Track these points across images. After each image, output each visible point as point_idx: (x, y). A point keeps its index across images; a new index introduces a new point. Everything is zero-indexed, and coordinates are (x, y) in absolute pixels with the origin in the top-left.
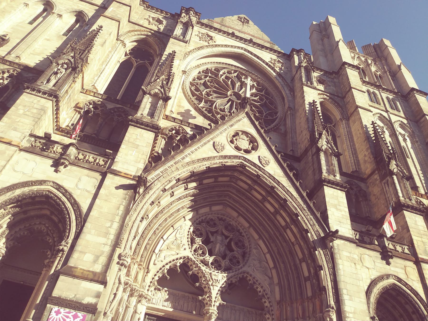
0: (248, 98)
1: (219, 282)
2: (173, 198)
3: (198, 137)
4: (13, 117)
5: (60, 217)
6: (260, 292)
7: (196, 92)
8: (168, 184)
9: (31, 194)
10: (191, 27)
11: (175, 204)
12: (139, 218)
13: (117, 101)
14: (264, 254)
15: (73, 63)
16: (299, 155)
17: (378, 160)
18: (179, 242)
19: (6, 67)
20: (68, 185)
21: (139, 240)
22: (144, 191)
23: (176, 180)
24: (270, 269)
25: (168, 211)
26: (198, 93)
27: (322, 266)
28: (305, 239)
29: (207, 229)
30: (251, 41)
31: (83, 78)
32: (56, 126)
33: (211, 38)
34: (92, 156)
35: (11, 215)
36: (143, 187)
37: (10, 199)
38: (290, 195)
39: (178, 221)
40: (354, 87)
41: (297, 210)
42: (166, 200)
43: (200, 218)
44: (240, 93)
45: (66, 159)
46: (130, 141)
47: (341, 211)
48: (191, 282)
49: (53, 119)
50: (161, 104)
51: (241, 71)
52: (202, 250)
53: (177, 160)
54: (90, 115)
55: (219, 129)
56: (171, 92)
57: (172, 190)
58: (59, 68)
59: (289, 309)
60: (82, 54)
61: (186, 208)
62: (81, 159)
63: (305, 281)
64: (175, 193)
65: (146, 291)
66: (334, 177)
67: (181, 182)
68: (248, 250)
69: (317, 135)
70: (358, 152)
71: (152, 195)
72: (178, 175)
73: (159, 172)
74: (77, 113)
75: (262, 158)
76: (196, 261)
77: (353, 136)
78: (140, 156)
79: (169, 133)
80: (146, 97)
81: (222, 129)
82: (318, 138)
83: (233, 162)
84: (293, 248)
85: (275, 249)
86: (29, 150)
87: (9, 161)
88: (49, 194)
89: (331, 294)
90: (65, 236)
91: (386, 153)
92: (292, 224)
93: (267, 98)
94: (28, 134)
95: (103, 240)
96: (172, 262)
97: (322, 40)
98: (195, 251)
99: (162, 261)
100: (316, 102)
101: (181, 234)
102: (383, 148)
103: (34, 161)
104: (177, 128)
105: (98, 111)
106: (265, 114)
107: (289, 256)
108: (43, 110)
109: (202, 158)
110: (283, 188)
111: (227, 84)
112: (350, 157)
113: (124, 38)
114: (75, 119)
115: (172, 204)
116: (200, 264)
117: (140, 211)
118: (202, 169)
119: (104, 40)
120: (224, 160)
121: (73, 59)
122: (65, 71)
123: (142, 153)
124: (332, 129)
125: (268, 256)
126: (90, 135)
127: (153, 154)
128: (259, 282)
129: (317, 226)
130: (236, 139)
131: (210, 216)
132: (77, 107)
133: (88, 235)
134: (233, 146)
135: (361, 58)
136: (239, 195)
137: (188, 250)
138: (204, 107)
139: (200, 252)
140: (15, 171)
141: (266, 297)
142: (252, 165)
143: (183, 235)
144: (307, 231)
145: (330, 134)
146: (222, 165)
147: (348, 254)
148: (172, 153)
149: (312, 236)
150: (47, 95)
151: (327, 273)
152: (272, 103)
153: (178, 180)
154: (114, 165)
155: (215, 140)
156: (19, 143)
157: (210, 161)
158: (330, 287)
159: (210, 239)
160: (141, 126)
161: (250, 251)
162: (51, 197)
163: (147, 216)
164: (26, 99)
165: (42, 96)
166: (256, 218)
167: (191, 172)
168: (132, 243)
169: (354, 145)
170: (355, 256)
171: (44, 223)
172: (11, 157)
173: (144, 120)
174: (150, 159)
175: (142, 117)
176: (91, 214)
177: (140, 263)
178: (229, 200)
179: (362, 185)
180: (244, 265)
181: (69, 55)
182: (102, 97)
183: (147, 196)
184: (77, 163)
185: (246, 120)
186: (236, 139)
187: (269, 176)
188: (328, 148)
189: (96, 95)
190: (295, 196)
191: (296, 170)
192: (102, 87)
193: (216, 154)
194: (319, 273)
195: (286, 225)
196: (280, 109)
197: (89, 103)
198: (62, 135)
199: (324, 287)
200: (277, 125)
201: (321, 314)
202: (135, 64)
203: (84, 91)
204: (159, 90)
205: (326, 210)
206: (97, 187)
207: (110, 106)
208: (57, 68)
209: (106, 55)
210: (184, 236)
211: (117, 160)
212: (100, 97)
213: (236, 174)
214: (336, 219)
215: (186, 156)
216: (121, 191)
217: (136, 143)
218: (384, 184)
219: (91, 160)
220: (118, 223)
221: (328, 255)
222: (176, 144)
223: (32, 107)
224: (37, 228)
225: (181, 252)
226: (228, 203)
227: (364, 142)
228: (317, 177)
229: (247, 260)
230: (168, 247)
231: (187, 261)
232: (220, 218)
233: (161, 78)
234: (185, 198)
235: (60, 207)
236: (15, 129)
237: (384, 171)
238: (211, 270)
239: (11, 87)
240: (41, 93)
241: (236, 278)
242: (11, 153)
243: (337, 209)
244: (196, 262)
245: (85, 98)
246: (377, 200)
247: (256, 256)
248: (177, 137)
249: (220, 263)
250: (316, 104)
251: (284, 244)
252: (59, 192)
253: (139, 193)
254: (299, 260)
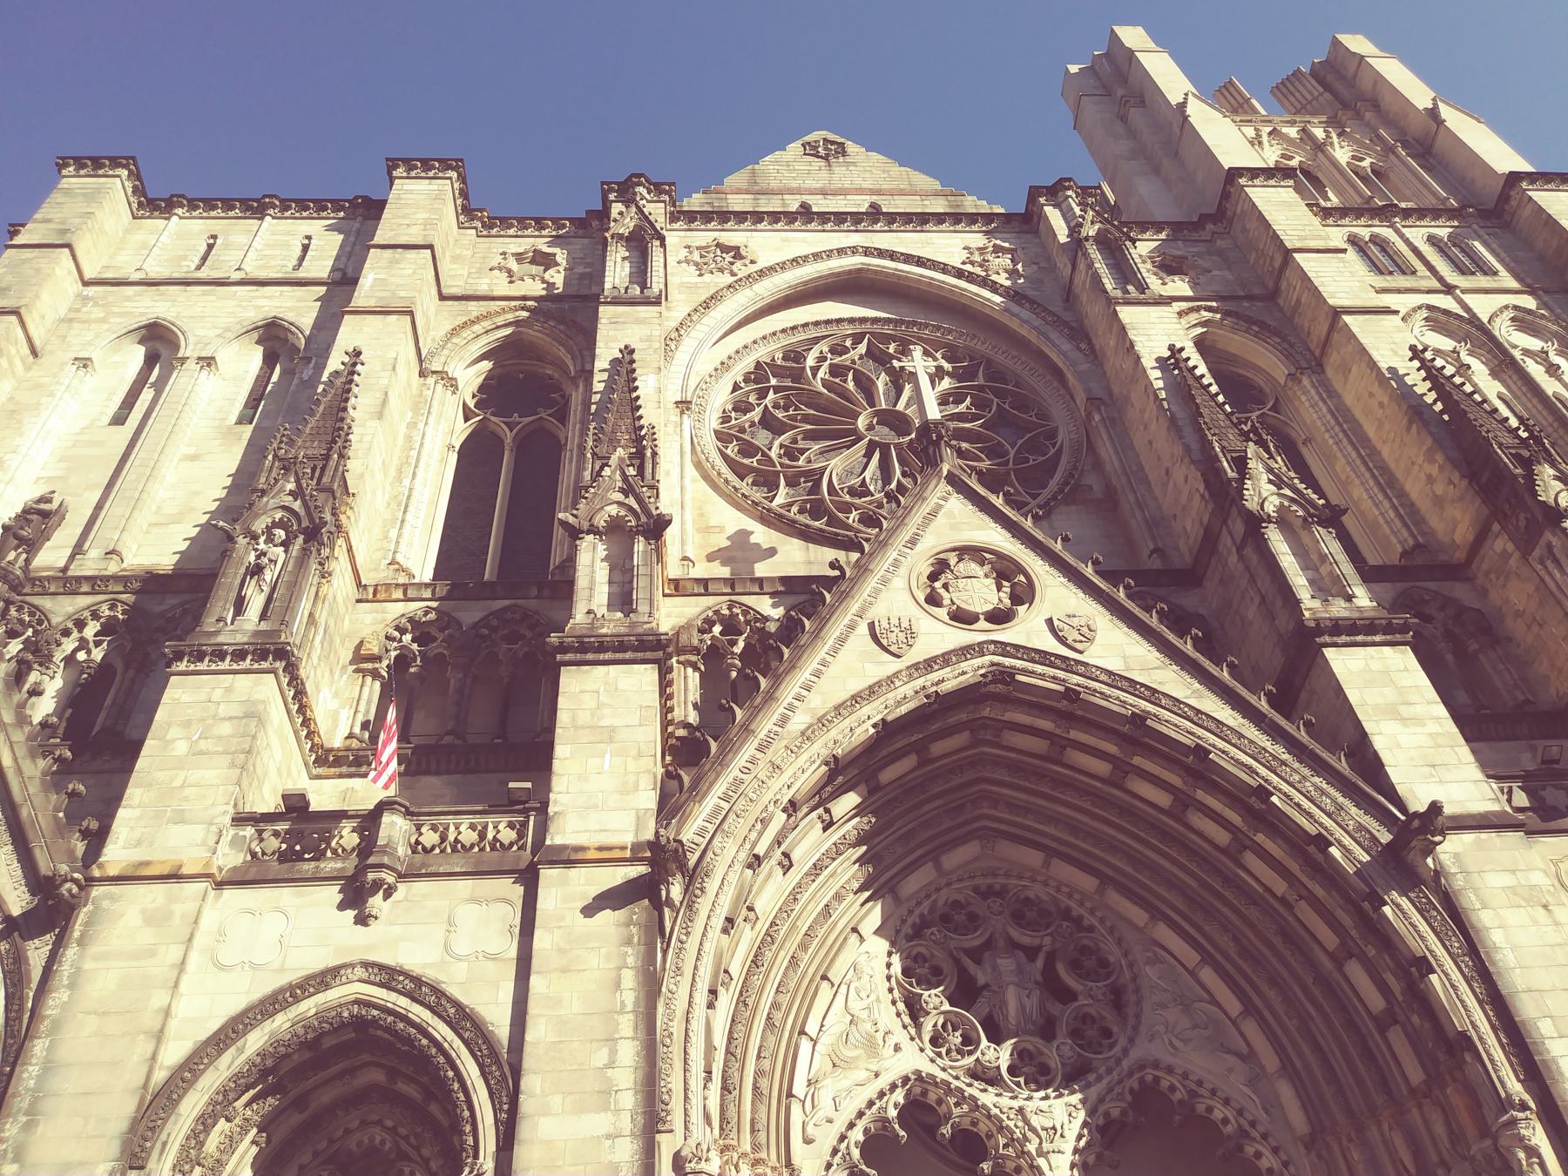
0: (936, 423)
1: (1062, 1136)
2: (795, 875)
3: (807, 623)
4: (160, 776)
5: (425, 1079)
6: (1225, 1121)
7: (746, 461)
8: (761, 834)
9: (301, 1031)
10: (658, 243)
11: (806, 895)
12: (701, 998)
13: (486, 591)
14: (1192, 973)
15: (302, 512)
16: (1188, 559)
17: (1484, 480)
18: (868, 1027)
19: (83, 601)
20: (415, 957)
21: (724, 1071)
22: (686, 890)
23: (784, 810)
24: (1234, 1022)
25: (793, 927)
26: (753, 462)
27: (1425, 957)
28: (1328, 873)
29: (953, 945)
30: (874, 216)
31: (350, 550)
32: (311, 750)
33: (737, 253)
34: (465, 821)
35: (255, 1130)
36: (679, 877)
37: (236, 1077)
38: (1212, 726)
39: (839, 950)
40: (1298, 245)
41: (1257, 774)
42: (771, 892)
43: (911, 912)
44: (900, 406)
45: (381, 866)
46: (580, 723)
47: (1418, 721)
48: (961, 1161)
49: (296, 733)
50: (645, 552)
51: (877, 328)
52: (960, 1032)
53: (762, 735)
54: (412, 670)
55: (872, 571)
56: (661, 496)
57: (783, 848)
58: (262, 546)
59: (1356, 1155)
60: (323, 469)
61: (852, 895)
62: (433, 848)
63: (1382, 1031)
64: (795, 856)
66: (1348, 605)
67: (805, 810)
68: (1127, 974)
69: (1229, 471)
70: (1399, 474)
71: (717, 895)
72: (785, 790)
73: (716, 800)
74: (369, 679)
75: (1061, 625)
76: (951, 1080)
77: (1356, 421)
78: (632, 765)
79: (701, 641)
80: (584, 544)
81: (885, 568)
82: (1237, 480)
83: (964, 673)
84: (1290, 919)
85: (1224, 940)
86: (247, 878)
87: (190, 940)
88: (364, 1013)
89: (1499, 1055)
90: (464, 1150)
91: (1507, 448)
92: (1257, 831)
93: (998, 393)
94: (227, 820)
95: (600, 1123)
96: (868, 1112)
97: (1123, 119)
98: (935, 1041)
99: (830, 1121)
100: (1182, 349)
101: (863, 995)
102: (1488, 431)
103: (277, 909)
104: (726, 612)
105: (435, 648)
106: (1012, 453)
107: (1287, 953)
108: (253, 715)
109: (848, 696)
110: (1175, 709)
111: (844, 394)
112: (1376, 505)
113: (443, 359)
114: (369, 702)
115: (798, 896)
116: (970, 1085)
117: (696, 968)
118: (863, 738)
119: (380, 395)
120: (929, 677)
121: (299, 502)
122: (286, 551)
123: (634, 753)
124: (1270, 421)
125: (1208, 975)
126: (432, 741)
127: (671, 735)
128: (1208, 1085)
129: (1354, 810)
130: (945, 586)
131: (945, 892)
132: (362, 660)
133: (542, 1119)
134: (942, 613)
135: (1285, 130)
136: (1026, 784)
137: (910, 1048)
138: (791, 504)
139: (956, 1039)
140: (222, 967)
141: (1254, 1134)
142: (1033, 661)
143: (873, 997)
144: (1322, 842)
145: (1276, 447)
146: (927, 697)
147: (1507, 880)
148: (739, 713)
149: (1348, 853)
150: (249, 657)
151: (1456, 976)
152: (1023, 405)
153: (792, 807)
154: (552, 828)
155: (871, 615)
156: (207, 864)
157: (882, 699)
158: (1485, 1027)
159: (973, 980)
160: (602, 657)
161: (1134, 979)
162: (374, 1021)
163: (726, 972)
164: (185, 698)
165: (235, 666)
166: (1114, 847)
167: (827, 763)
168: (705, 1098)
169: (1374, 453)
170: (1538, 878)
171: (375, 1117)
172: (196, 922)
173: (604, 631)
174: (668, 758)
175: (592, 624)
176: (529, 1037)
177: (757, 1156)
178: (992, 812)
179: (1460, 591)
180: (1131, 1040)
181: (281, 490)
182: (433, 593)
183: (703, 905)
184: (423, 865)
185: (957, 505)
186: (945, 586)
187: (1109, 681)
188: (1286, 504)
189: (411, 593)
190: (1231, 722)
191: (1200, 621)
192: (422, 560)
193: (893, 665)
194: (1422, 986)
195: (1235, 839)
196: (1059, 414)
197: (397, 628)
198: (341, 776)
199: (1464, 1038)
200: (1071, 475)
201: (1488, 1142)
202: (509, 437)
203: (369, 594)
204: (619, 503)
205: (1363, 738)
206: (517, 930)
207: (470, 614)
208: (256, 550)
209: (401, 440)
210: (878, 1000)
211: (556, 809)
212: (427, 594)
213: (986, 712)
214: (1412, 759)
215: (791, 708)
216: (607, 916)
218: (1542, 562)
219: (468, 837)
220: (633, 1039)
221: (1435, 908)
222: (739, 671)
223: (214, 717)
224: (359, 1144)
225: (886, 1064)
226: (995, 825)
227: (1408, 429)
228: (1284, 623)
229: (1138, 1016)
230: (837, 1062)
231: (918, 1090)
232: (983, 888)
233: (614, 460)
234: (834, 859)
235: (414, 1047)
236: (180, 818)
237: (1522, 516)
238: (1016, 1097)
239: (119, 666)
240: (228, 658)
241: (1120, 1097)
242: (191, 906)
243: (1404, 720)
244: (955, 1083)
245: (380, 616)
246: (1535, 628)
247: (1165, 990)
248: (733, 643)
249: (1042, 1059)
250: (1184, 355)
251: (1253, 913)
252: (394, 995)
253: (669, 902)
254: (1331, 956)
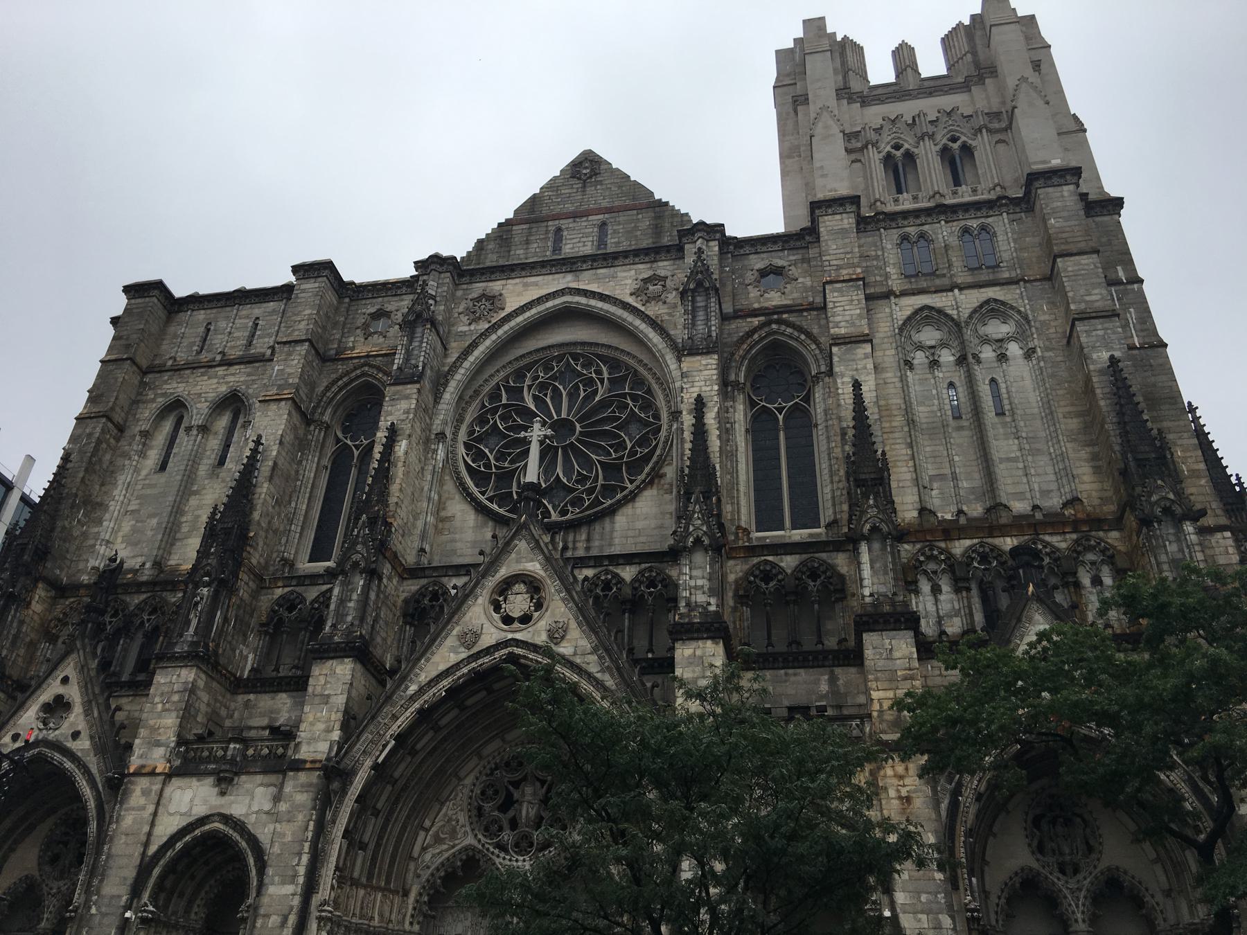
4: (151, 722)
8: (381, 752)
18: (454, 823)
19: (143, 597)
65: (407, 926)
93: (635, 398)
95: (289, 889)
106: (629, 446)
119: (271, 463)
152: (648, 405)
159: (512, 795)
186: (505, 600)
202: (356, 453)
217: (326, 693)
236: (158, 744)
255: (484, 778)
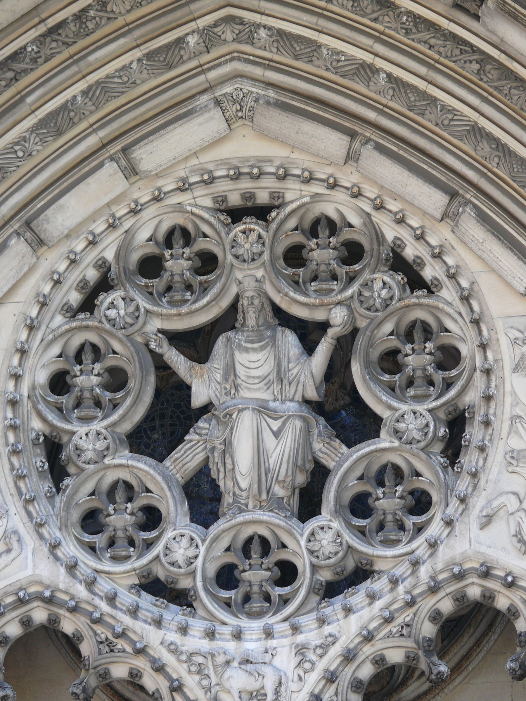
29: (156, 324)
161: (488, 398)
255: (59, 319)
